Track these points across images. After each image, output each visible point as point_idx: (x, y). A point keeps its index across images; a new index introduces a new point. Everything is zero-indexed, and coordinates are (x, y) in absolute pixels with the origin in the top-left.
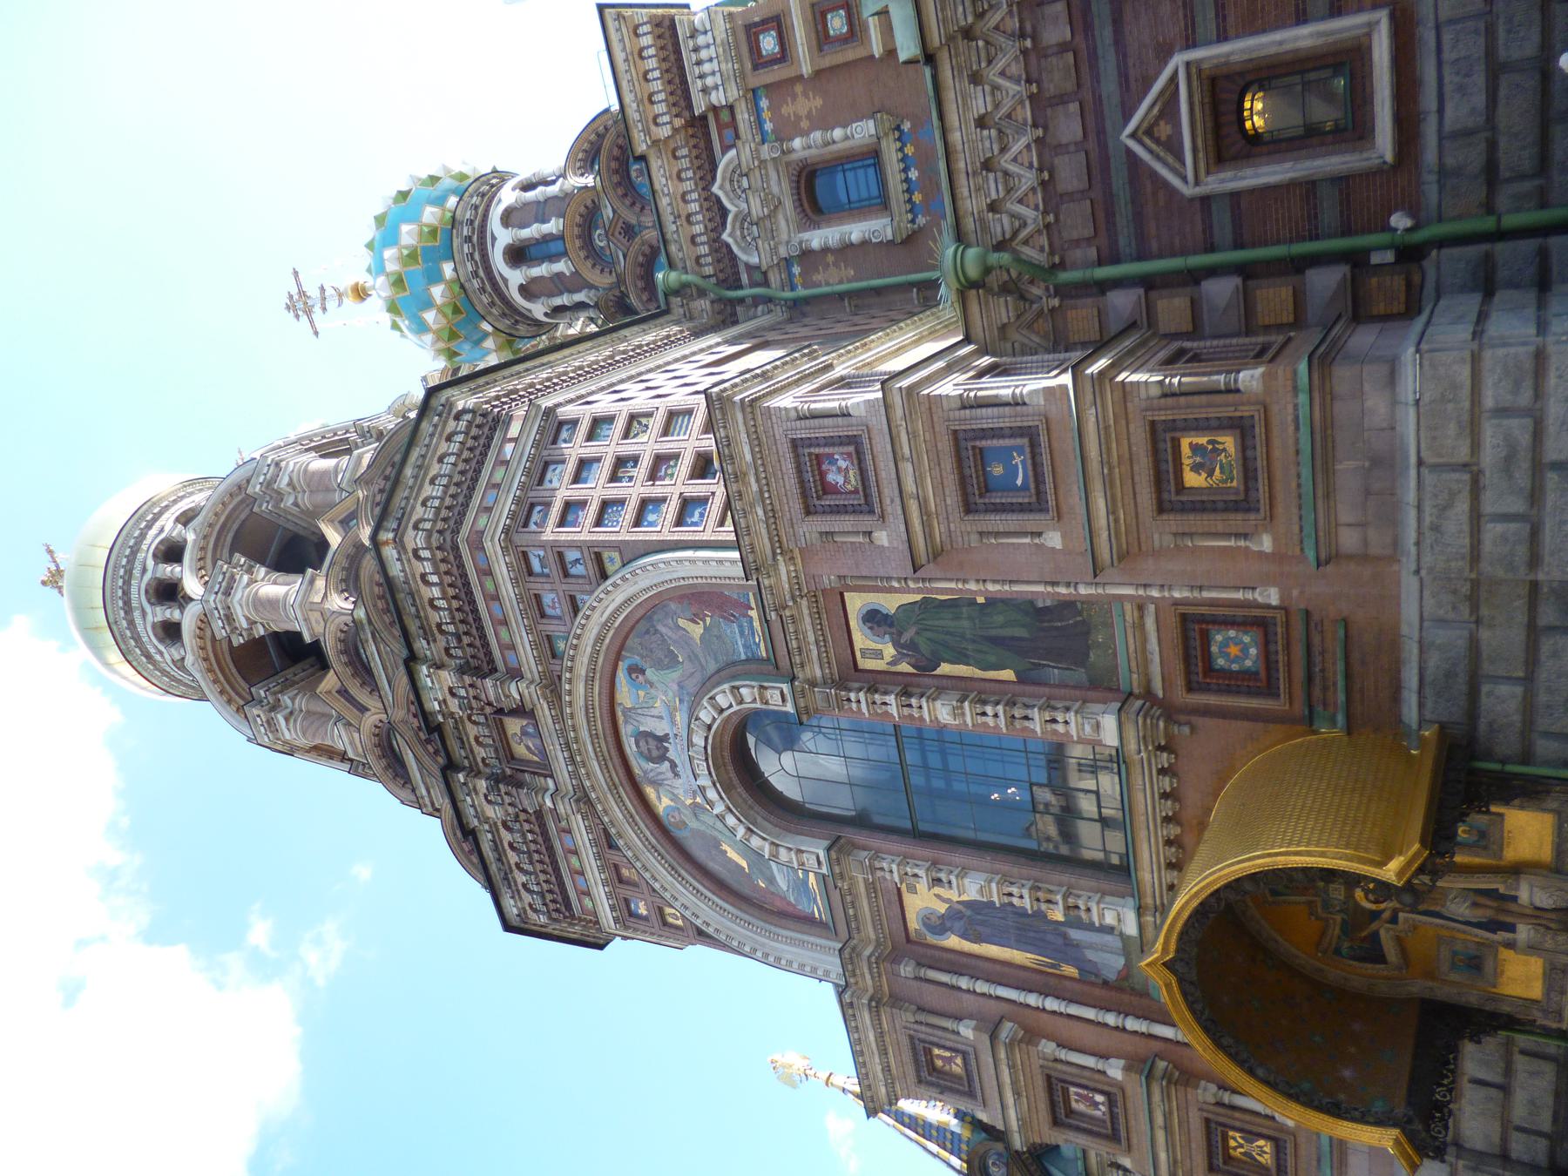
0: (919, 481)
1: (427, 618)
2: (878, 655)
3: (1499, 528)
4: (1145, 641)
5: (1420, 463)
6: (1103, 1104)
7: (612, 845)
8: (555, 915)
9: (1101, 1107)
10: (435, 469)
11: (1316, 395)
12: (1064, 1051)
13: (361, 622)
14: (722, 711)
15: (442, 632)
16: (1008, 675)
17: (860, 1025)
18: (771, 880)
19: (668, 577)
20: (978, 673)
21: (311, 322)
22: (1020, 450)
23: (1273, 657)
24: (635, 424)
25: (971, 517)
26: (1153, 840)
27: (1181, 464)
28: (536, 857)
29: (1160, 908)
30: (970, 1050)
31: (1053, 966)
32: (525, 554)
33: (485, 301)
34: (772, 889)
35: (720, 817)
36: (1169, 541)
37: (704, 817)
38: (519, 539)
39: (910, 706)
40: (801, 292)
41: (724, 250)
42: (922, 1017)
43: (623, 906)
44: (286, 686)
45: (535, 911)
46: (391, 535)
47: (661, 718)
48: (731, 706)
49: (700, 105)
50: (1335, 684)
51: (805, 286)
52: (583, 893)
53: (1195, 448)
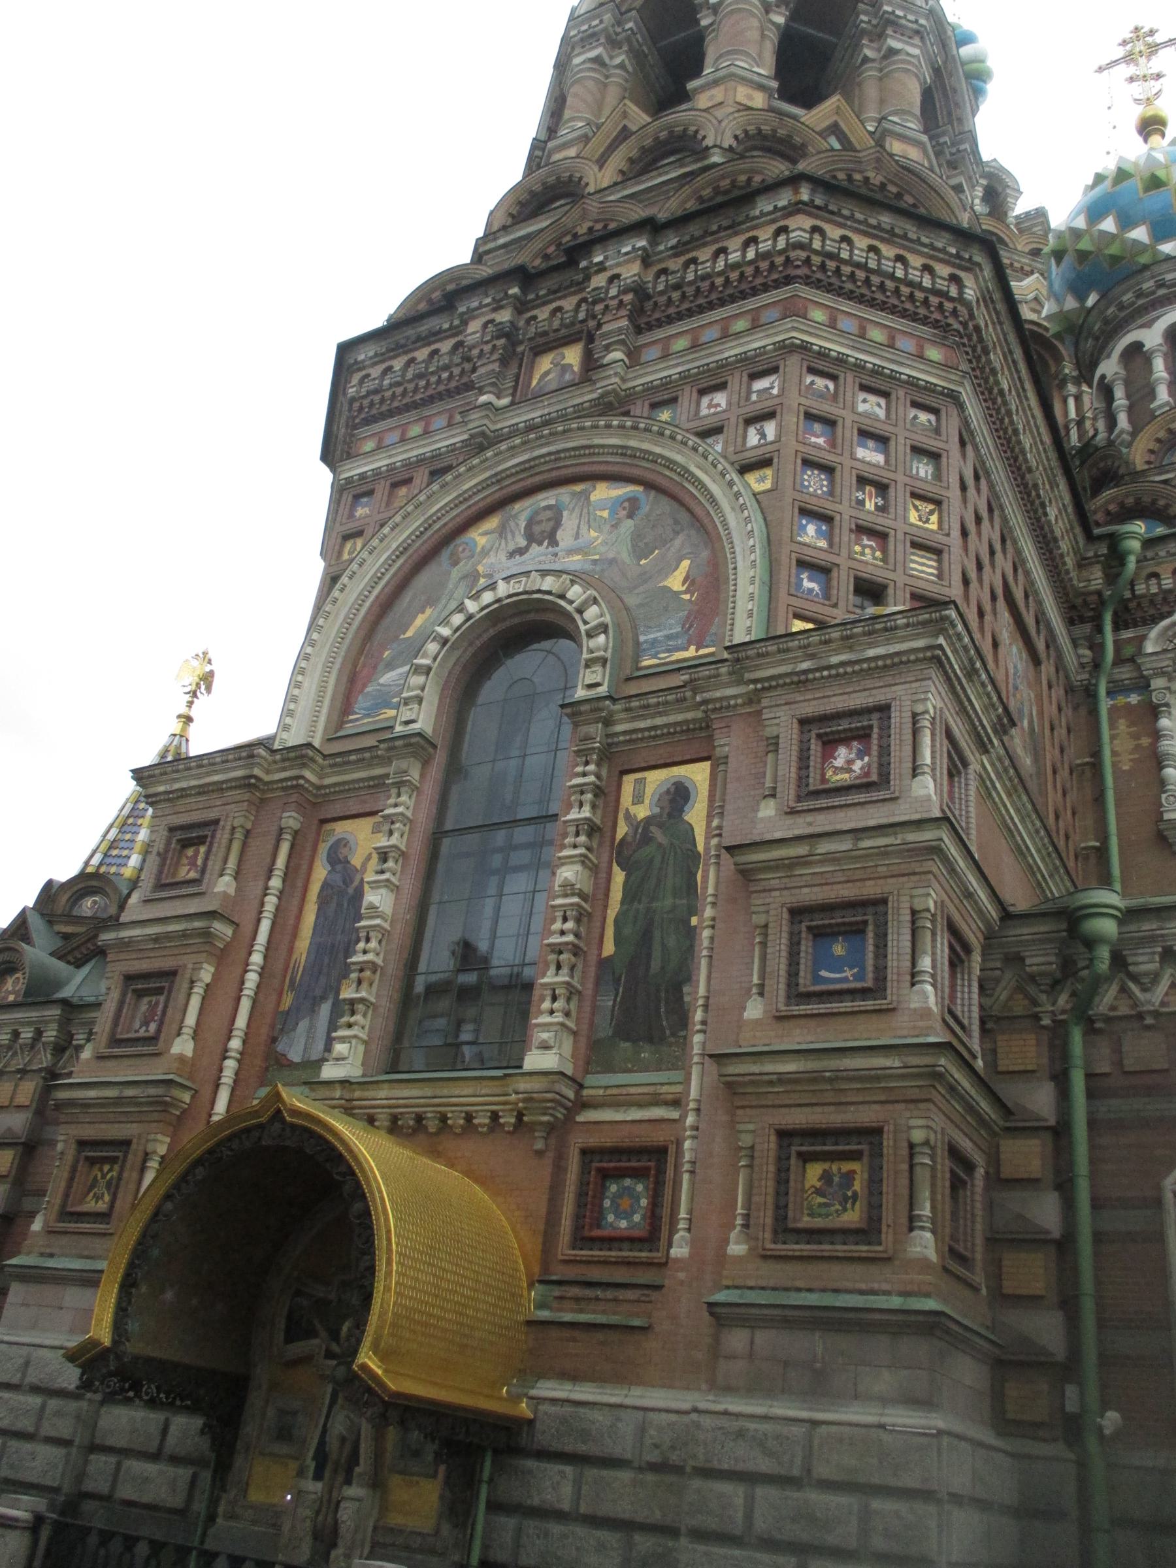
0: (830, 858)
1: (705, 245)
3: (739, 1501)
4: (641, 1105)
5: (815, 1423)
6: (147, 1031)
7: (436, 474)
8: (356, 405)
10: (888, 251)
12: (201, 991)
13: (705, 158)
14: (580, 611)
15: (686, 265)
16: (609, 948)
17: (229, 765)
18: (390, 666)
19: (738, 549)
20: (612, 914)
21: (1114, 63)
22: (860, 977)
23: (616, 1245)
24: (931, 507)
25: (786, 915)
26: (422, 1101)
27: (832, 1161)
28: (422, 383)
29: (348, 1105)
30: (203, 888)
32: (774, 370)
33: (1125, 298)
34: (381, 667)
35: (461, 608)
36: (746, 1140)
38: (793, 364)
40: (1105, 704)
41: (1166, 609)
42: (239, 835)
43: (365, 488)
44: (637, 56)
45: (362, 381)
46: (805, 197)
47: (577, 536)
48: (585, 623)
50: (581, 1311)
51: (1112, 710)
52: (380, 440)
53: (849, 1176)
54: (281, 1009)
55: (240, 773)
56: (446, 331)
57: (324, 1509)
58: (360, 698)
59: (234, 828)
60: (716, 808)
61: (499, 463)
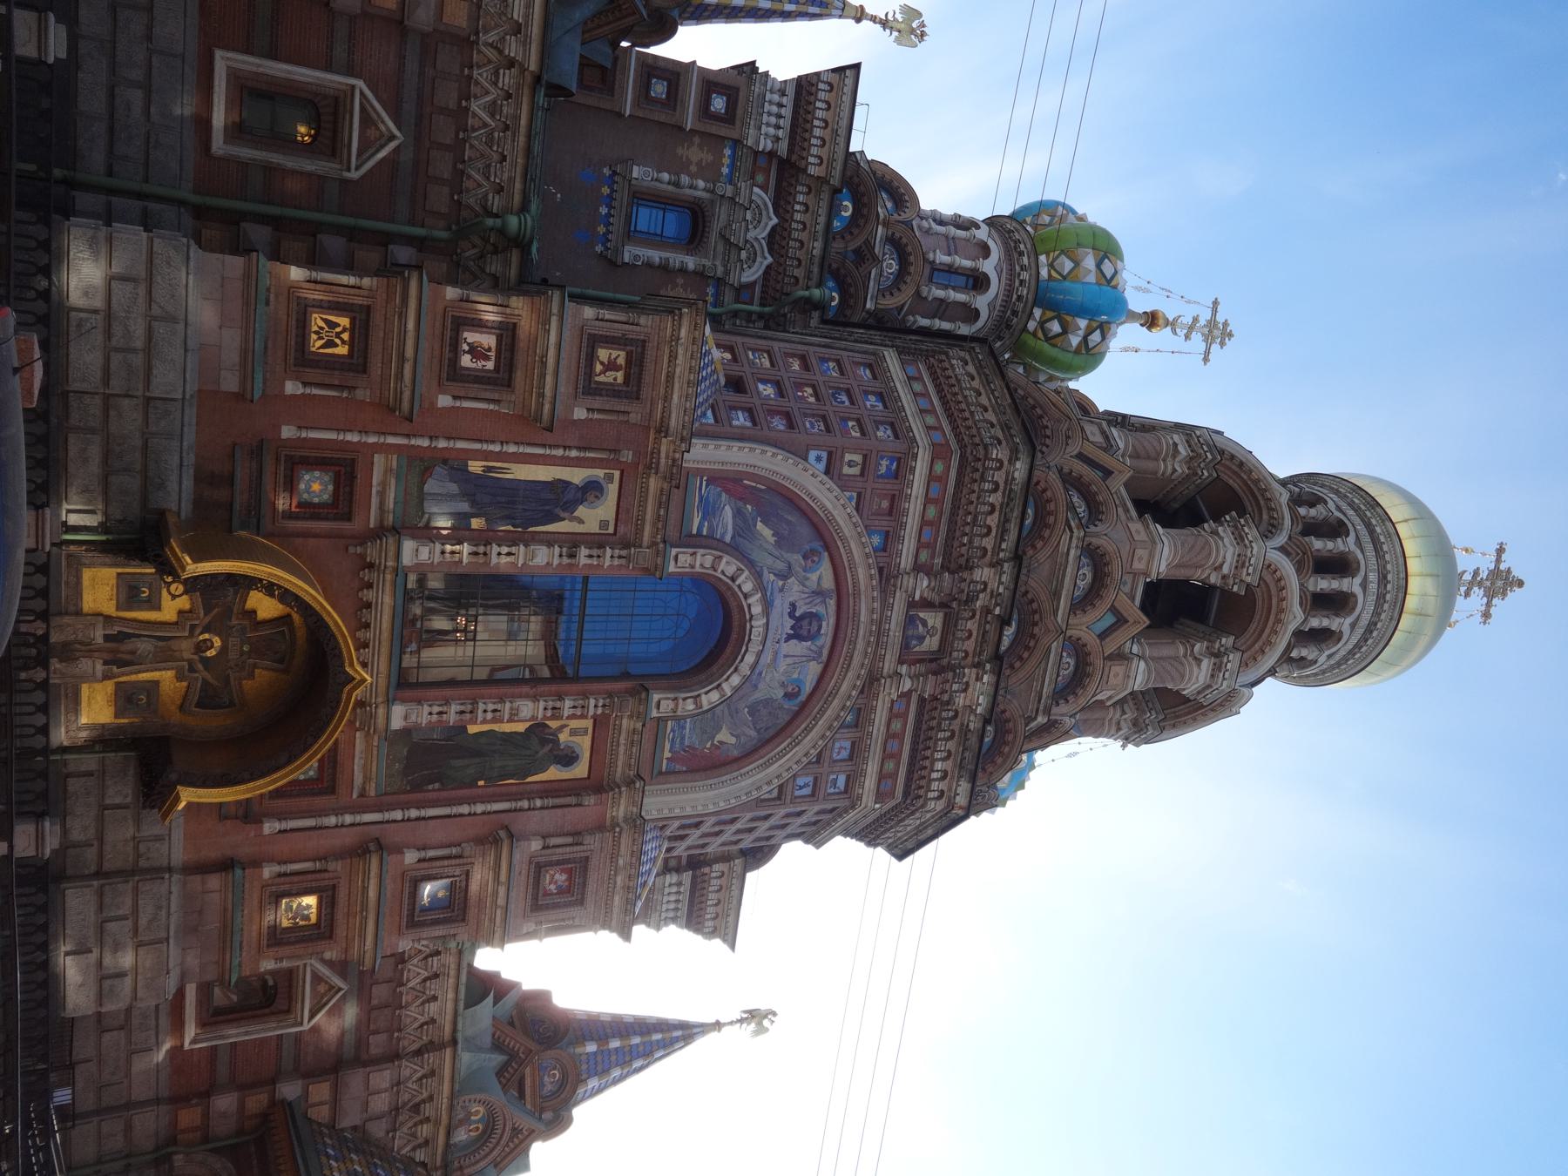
2: (574, 732)
3: (121, 912)
5: (167, 939)
6: (464, 352)
8: (981, 455)
9: (466, 347)
11: (228, 966)
16: (472, 729)
18: (738, 513)
31: (490, 469)
32: (846, 791)
34: (740, 504)
37: (780, 566)
39: (554, 708)
47: (785, 656)
49: (687, 877)
54: (470, 463)
55: (673, 423)
56: (1000, 543)
57: (83, 648)
58: (719, 489)
59: (628, 413)
60: (552, 790)
61: (866, 597)
